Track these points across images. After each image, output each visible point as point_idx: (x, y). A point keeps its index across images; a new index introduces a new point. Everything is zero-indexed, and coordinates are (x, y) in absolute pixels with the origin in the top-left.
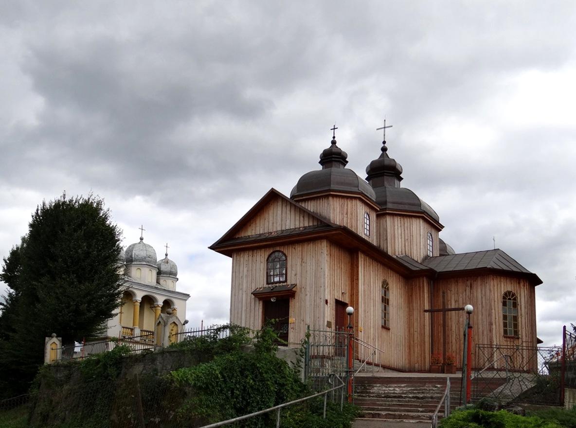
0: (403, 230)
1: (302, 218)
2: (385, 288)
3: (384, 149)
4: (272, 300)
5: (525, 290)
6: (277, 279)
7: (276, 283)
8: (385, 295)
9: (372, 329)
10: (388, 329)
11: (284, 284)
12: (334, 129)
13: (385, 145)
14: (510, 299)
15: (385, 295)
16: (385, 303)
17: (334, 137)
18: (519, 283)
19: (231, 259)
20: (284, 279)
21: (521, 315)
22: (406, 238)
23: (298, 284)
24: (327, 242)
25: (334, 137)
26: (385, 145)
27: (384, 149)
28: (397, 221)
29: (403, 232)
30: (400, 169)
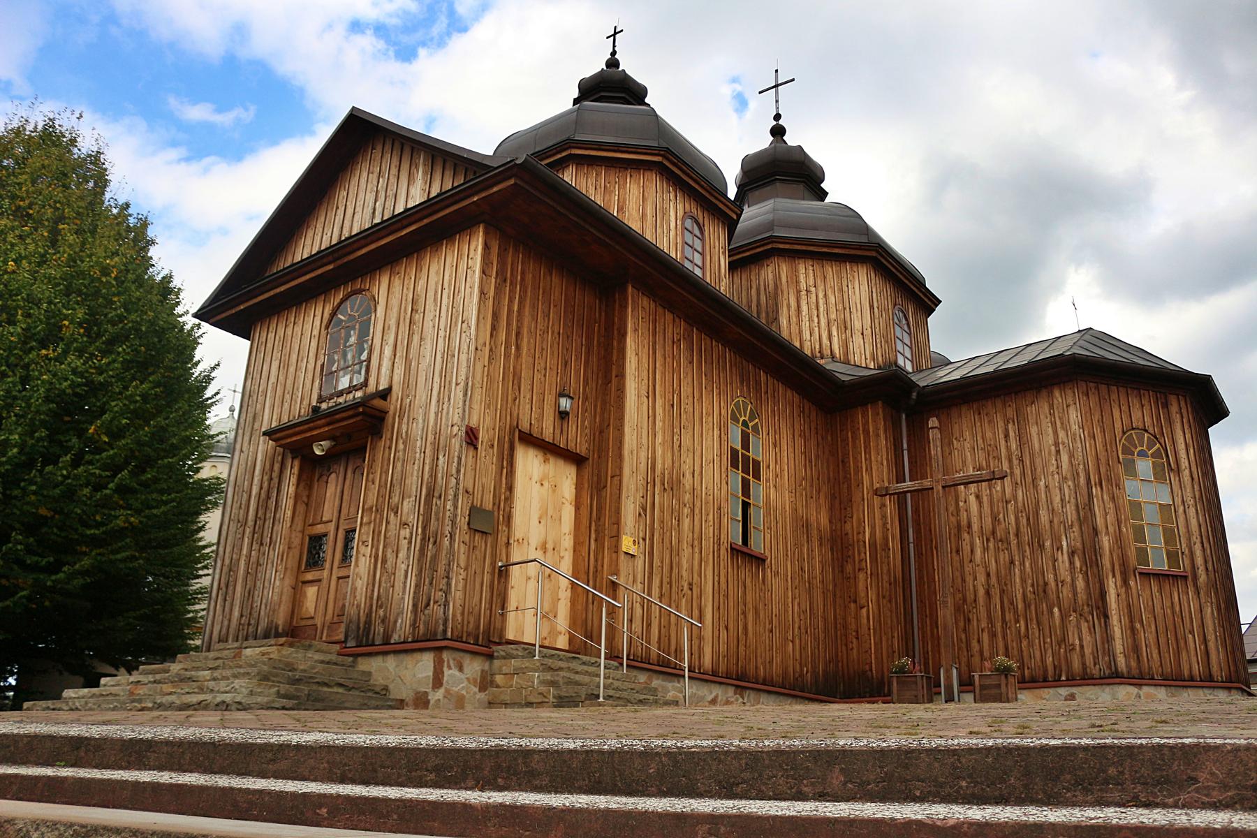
0: (821, 295)
1: (405, 166)
2: (745, 423)
3: (778, 132)
4: (318, 452)
5: (1186, 427)
6: (344, 383)
7: (341, 394)
8: (745, 445)
9: (686, 552)
10: (760, 560)
11: (359, 394)
12: (616, 33)
13: (781, 122)
14: (1142, 454)
15: (745, 445)
16: (746, 471)
17: (614, 53)
18: (1166, 405)
19: (246, 344)
20: (362, 380)
21: (1183, 502)
22: (833, 316)
23: (395, 388)
24: (486, 233)
25: (614, 53)
26: (781, 122)
27: (778, 132)
28: (806, 273)
29: (821, 302)
30: (819, 174)
